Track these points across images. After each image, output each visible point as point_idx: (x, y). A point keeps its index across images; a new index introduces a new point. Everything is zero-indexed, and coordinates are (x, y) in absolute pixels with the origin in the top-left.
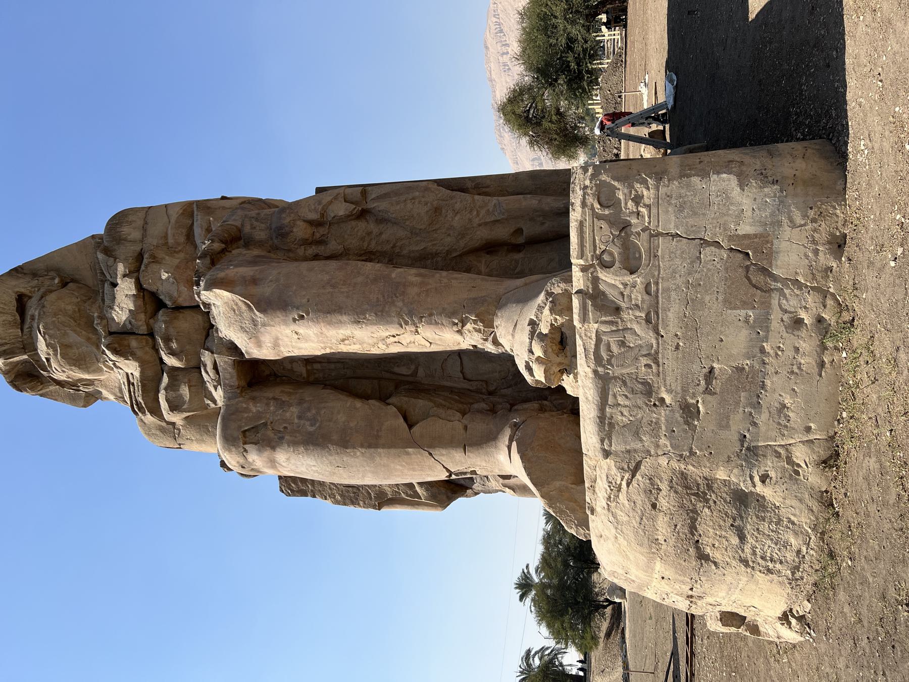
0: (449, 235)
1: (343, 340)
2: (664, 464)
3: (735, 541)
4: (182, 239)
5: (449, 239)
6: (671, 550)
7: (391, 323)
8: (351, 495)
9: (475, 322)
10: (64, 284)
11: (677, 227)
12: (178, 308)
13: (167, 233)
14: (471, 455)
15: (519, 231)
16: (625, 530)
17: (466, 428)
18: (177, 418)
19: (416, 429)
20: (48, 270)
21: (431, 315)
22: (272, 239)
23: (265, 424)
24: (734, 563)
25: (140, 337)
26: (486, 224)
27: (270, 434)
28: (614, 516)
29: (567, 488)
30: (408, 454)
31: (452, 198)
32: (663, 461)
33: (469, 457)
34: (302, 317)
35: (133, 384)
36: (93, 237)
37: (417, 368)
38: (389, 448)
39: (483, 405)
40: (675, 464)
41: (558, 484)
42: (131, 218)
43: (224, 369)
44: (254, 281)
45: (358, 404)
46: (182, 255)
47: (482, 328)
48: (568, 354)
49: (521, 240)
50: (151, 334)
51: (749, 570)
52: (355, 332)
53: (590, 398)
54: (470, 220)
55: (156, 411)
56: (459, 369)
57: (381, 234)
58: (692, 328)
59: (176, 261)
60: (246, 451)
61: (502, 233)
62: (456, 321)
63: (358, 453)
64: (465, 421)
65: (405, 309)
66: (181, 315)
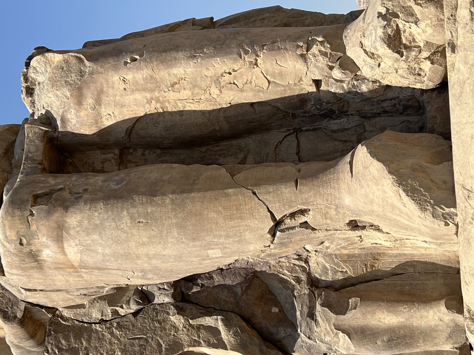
1: (173, 85)
7: (231, 53)
9: (322, 43)
21: (274, 42)
27: (66, 194)
29: (421, 166)
30: (227, 195)
33: (301, 192)
34: (134, 60)
38: (206, 190)
41: (410, 162)
43: (30, 141)
47: (329, 51)
52: (189, 70)
56: (295, 151)
60: (32, 214)
62: (301, 44)
63: (168, 201)
65: (246, 41)
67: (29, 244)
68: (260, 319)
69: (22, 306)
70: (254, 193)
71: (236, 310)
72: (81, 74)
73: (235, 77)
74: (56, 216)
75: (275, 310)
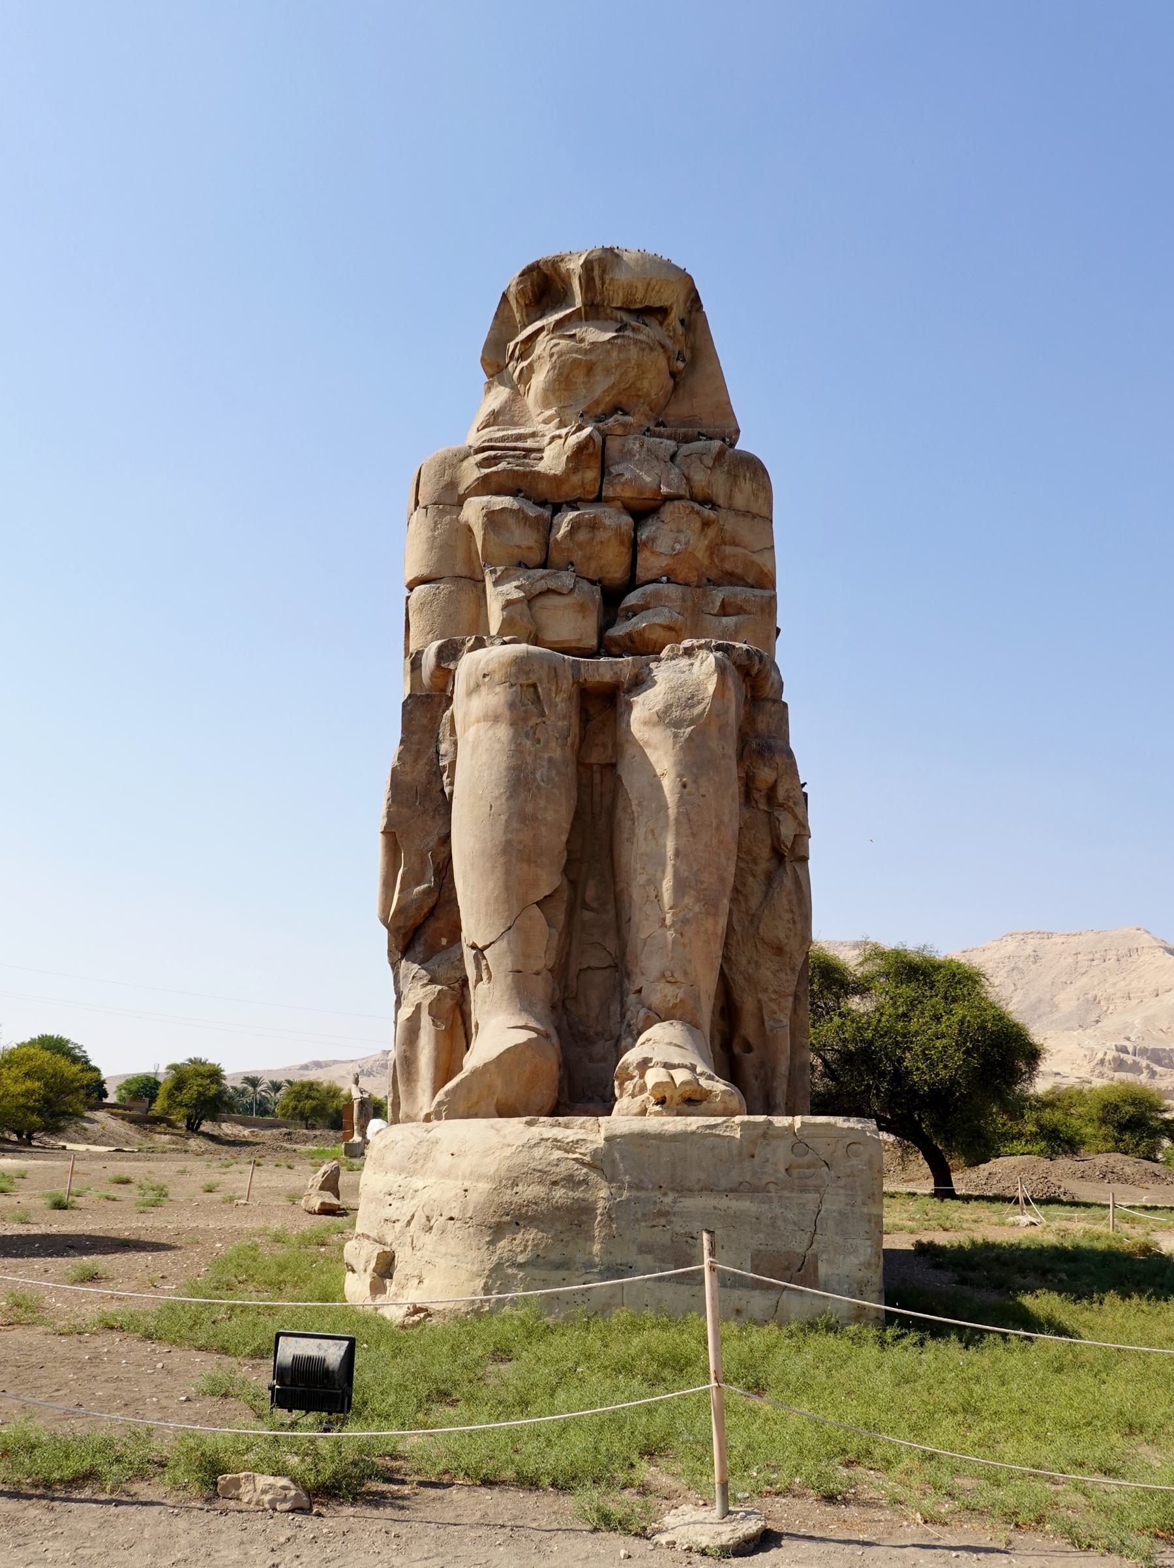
0: (749, 962)
1: (653, 832)
2: (601, 1194)
3: (521, 1259)
4: (728, 566)
5: (744, 961)
6: (506, 1198)
8: (419, 802)
10: (673, 375)
11: (826, 1210)
12: (634, 547)
13: (737, 545)
14: (510, 978)
15: (748, 1048)
16: (523, 1154)
17: (537, 973)
18: (473, 511)
19: (536, 911)
22: (756, 737)
23: (542, 714)
24: (495, 1258)
25: (598, 485)
26: (760, 1009)
27: (534, 720)
28: (537, 1145)
31: (793, 969)
32: (603, 1193)
33: (506, 976)
34: (684, 786)
35: (525, 457)
36: (738, 431)
37: (592, 910)
40: (601, 1204)
41: (499, 1083)
42: (762, 495)
44: (722, 728)
46: (706, 562)
48: (679, 1107)
49: (737, 1050)
50: (599, 499)
51: (486, 1272)
53: (666, 1127)
54: (766, 990)
55: (485, 486)
56: (593, 964)
57: (754, 876)
58: (733, 1221)
59: (700, 555)
61: (749, 1029)
64: (545, 972)
66: (625, 550)
67: (484, 684)
68: (433, 925)
69: (452, 667)
70: (510, 928)
71: (441, 901)
72: (677, 724)
73: (652, 902)
74: (507, 713)
75: (444, 941)
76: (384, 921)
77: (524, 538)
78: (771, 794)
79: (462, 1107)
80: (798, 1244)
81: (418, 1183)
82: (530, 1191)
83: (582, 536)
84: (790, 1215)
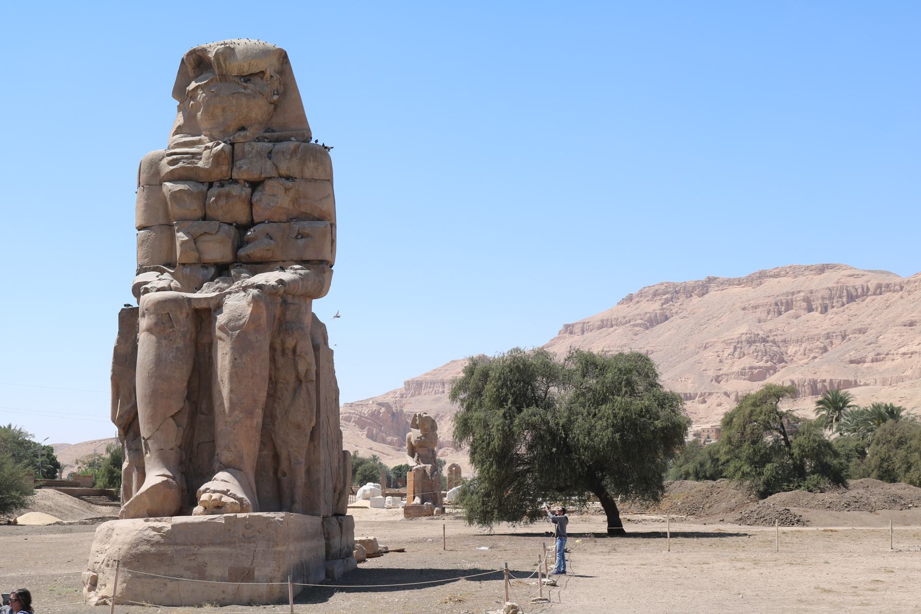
4: (303, 209)
15: (284, 474)
19: (171, 420)
20: (285, 85)
23: (173, 327)
31: (305, 435)
35: (192, 158)
39: (184, 456)
45: (185, 384)
49: (280, 475)
61: (284, 465)
76: (114, 421)
77: (193, 208)
78: (294, 351)
79: (132, 513)
80: (247, 564)
81: (107, 547)
82: (144, 548)
83: (222, 202)
84: (244, 552)
